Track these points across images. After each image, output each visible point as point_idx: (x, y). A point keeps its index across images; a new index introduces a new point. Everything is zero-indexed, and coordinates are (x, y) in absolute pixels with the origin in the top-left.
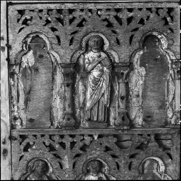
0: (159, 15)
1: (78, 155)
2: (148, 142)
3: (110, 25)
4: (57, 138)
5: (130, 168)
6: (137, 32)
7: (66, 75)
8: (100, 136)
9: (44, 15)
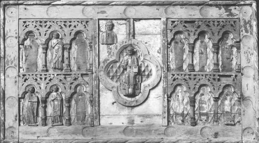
0: (82, 24)
1: (48, 83)
2: (78, 77)
3: (61, 28)
4: (39, 76)
5: (70, 89)
6: (73, 31)
7: (43, 48)
8: (57, 75)
9: (34, 24)
